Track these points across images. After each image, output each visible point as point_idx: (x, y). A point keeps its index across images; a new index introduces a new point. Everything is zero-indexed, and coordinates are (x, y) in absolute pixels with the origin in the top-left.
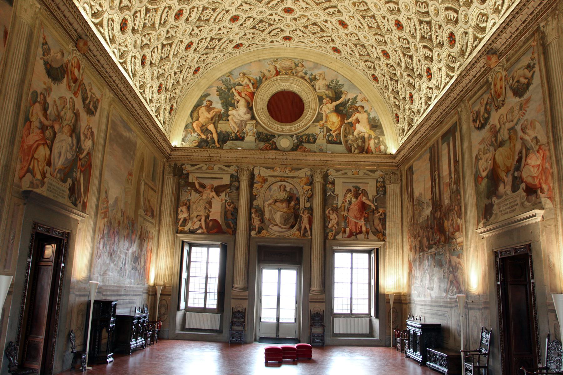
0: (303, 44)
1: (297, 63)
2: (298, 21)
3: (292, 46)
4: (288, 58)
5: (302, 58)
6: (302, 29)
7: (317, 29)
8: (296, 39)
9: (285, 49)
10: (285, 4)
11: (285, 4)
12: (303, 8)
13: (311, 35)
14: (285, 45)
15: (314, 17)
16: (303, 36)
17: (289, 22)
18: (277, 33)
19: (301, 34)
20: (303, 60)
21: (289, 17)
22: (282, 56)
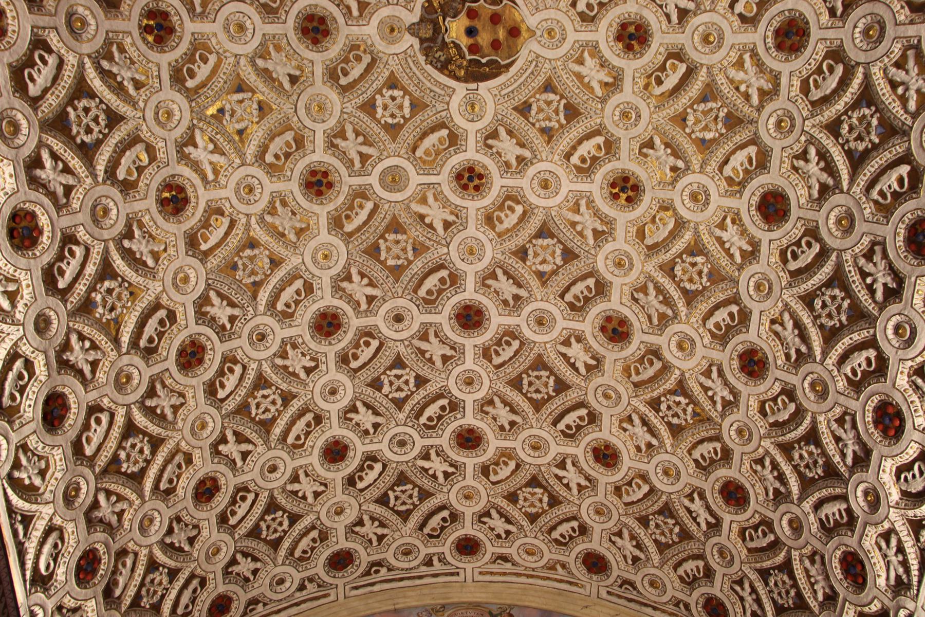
0: (509, 565)
1: (494, 613)
2: (493, 478)
3: (481, 578)
4: (470, 603)
5: (509, 602)
6: (504, 503)
7: (541, 501)
8: (488, 544)
9: (462, 587)
10: (459, 416)
11: (459, 416)
12: (499, 536)
13: (525, 523)
14: (461, 578)
15: (532, 452)
16: (508, 533)
17: (469, 481)
18: (443, 528)
19: (500, 525)
20: (511, 606)
21: (471, 461)
22: (456, 600)
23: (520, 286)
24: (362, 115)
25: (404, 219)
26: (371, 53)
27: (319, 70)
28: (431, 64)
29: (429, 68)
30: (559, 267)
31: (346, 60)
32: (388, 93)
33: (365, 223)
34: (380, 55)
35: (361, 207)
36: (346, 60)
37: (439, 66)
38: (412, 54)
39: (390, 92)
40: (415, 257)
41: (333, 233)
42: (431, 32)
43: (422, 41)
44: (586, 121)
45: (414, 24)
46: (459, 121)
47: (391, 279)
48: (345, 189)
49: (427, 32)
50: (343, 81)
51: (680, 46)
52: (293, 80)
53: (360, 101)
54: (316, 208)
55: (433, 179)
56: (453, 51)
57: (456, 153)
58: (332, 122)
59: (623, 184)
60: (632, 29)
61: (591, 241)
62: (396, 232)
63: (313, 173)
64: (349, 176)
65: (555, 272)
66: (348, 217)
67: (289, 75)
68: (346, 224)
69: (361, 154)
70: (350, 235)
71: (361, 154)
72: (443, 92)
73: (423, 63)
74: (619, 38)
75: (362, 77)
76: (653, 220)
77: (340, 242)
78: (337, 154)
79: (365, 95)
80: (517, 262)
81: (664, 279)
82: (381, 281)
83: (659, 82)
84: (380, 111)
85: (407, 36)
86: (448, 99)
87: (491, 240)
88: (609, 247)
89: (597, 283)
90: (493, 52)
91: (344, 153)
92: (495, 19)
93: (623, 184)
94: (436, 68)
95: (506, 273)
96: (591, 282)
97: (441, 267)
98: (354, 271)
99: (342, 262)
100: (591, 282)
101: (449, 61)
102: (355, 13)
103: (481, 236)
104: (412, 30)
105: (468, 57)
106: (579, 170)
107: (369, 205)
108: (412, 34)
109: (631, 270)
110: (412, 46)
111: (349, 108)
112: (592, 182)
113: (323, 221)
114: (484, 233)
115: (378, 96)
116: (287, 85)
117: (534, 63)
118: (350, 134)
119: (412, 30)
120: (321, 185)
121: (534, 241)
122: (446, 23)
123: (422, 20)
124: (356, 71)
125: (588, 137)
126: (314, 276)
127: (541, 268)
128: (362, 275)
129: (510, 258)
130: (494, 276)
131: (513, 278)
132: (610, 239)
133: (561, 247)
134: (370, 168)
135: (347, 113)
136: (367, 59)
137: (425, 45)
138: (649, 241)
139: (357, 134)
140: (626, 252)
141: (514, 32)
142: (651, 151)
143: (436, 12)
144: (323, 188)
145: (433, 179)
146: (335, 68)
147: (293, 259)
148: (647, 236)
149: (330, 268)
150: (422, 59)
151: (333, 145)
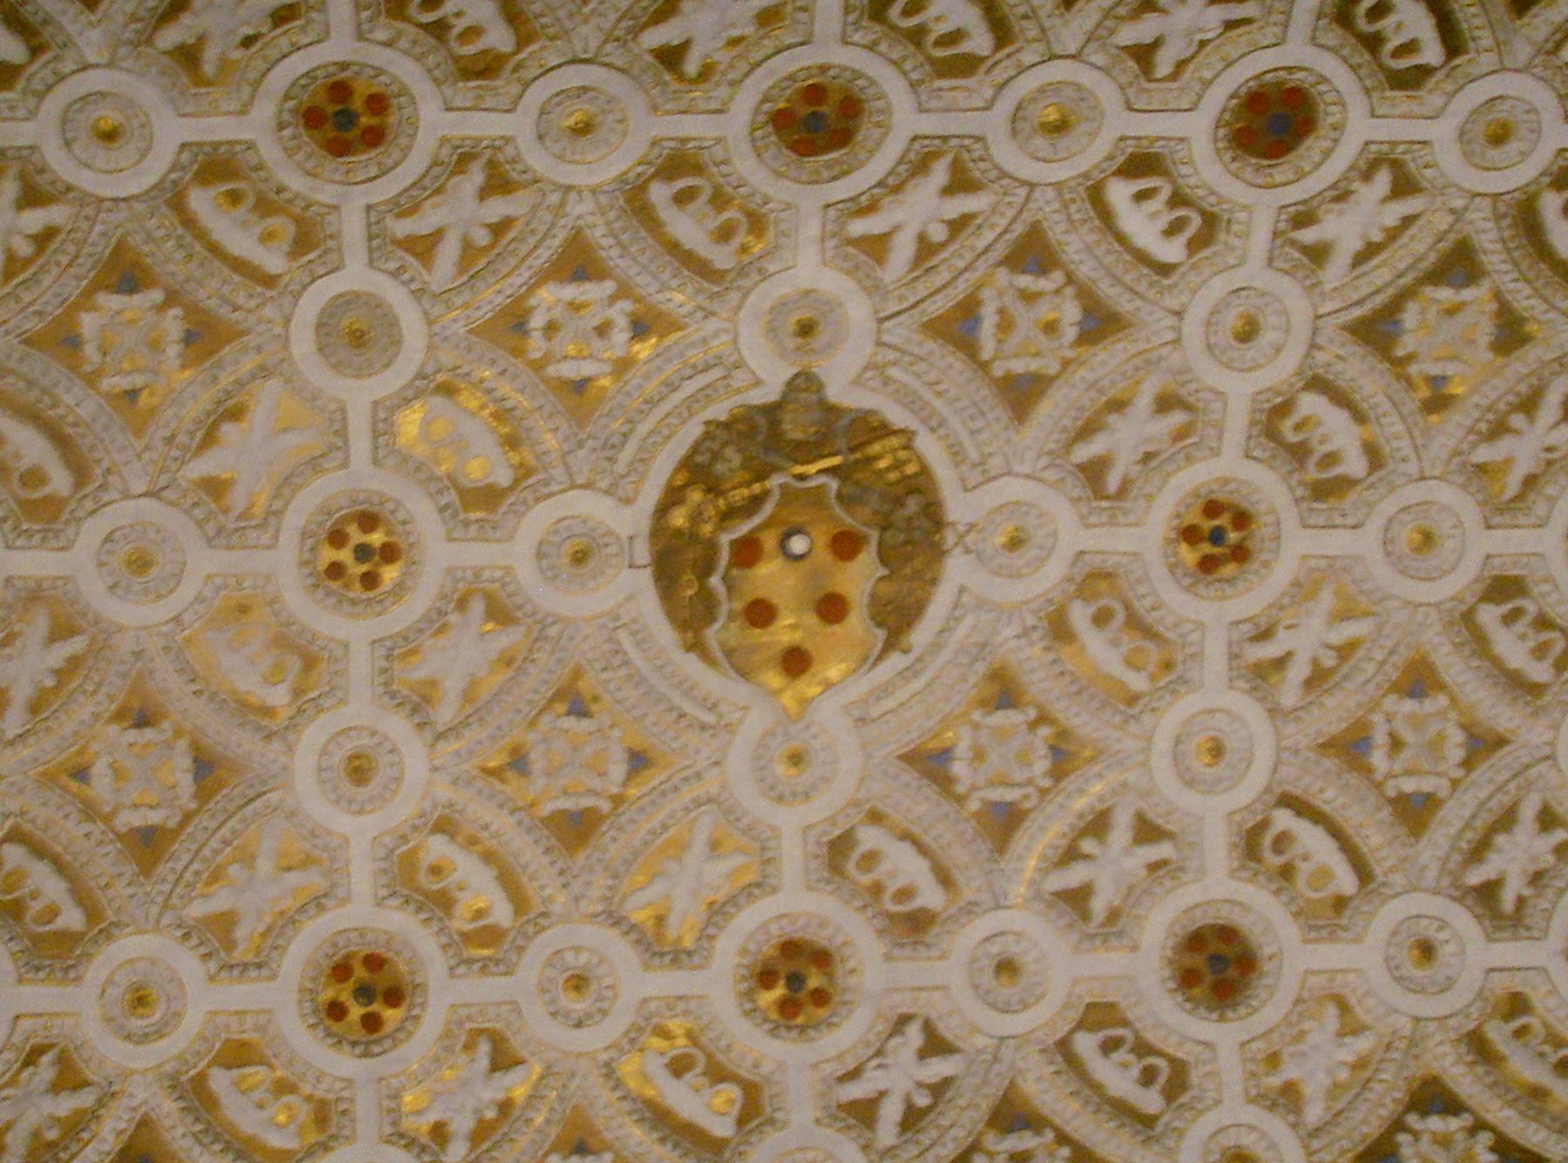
23: (34, 708)
24: (556, 242)
25: (237, 363)
26: (742, 272)
27: (693, 127)
28: (707, 436)
29: (694, 431)
30: (108, 819)
31: (720, 200)
32: (620, 314)
33: (216, 250)
34: (734, 297)
35: (267, 237)
36: (720, 200)
37: (699, 459)
38: (735, 384)
39: (622, 322)
40: (110, 397)
41: (185, 157)
42: (798, 435)
43: (772, 411)
44: (554, 871)
45: (820, 388)
46: (537, 521)
47: (33, 325)
48: (326, 194)
49: (794, 428)
50: (659, 193)
51: (779, 1115)
52: (671, 57)
53: (598, 235)
54: (266, 110)
55: (360, 446)
56: (740, 495)
57: (442, 510)
58: (537, 160)
59: (380, 988)
60: (814, 981)
61: (197, 910)
62: (189, 339)
63: (378, 103)
64: (369, 208)
65: (90, 811)
66: (235, 198)
67: (685, 46)
68: (212, 192)
69: (437, 235)
70: (178, 204)
71: (437, 235)
72: (621, 467)
73: (708, 414)
74: (790, 948)
75: (674, 248)
76: (283, 1088)
77: (152, 179)
78: (437, 170)
79: (614, 252)
80: (112, 699)
81: (111, 1138)
82: (27, 298)
83: (678, 1068)
84: (570, 292)
85: (786, 372)
86: (604, 484)
87: (177, 619)
88: (188, 964)
89: (68, 939)
90: (738, 605)
91: (438, 191)
92: (832, 608)
93: (380, 988)
94: (695, 449)
95: (74, 663)
96: (71, 918)
97: (81, 474)
98: (55, 215)
99: (88, 181)
100: (71, 918)
101: (714, 489)
102: (858, 227)
103: (188, 590)
104: (804, 383)
105: (725, 539)
106: (408, 863)
107: (273, 261)
108: (791, 384)
109: (128, 1037)
110: (758, 383)
111: (580, 208)
112: (380, 903)
113: (220, 128)
114: (199, 599)
115: (609, 287)
116: (656, 37)
117: (709, 718)
118: (497, 208)
119: (804, 383)
120: (339, 126)
121: (182, 744)
122: (822, 479)
123: (831, 410)
124: (689, 228)
125: (509, 881)
126: (41, 96)
127: (100, 769)
128: (44, 238)
129: (124, 675)
130: (60, 631)
131: (56, 689)
132: (213, 965)
133: (172, 824)
134: (392, 266)
135: (562, 204)
136: (722, 257)
137: (762, 422)
138: (220, 1081)
139: (499, 229)
140: (178, 1015)
141: (796, 662)
142: (484, 1062)
143: (852, 450)
144: (329, 131)
145: (360, 446)
146: (698, 169)
147: (95, 35)
148: (235, 1073)
149: (68, 144)
150: (720, 410)
151: (464, 160)
